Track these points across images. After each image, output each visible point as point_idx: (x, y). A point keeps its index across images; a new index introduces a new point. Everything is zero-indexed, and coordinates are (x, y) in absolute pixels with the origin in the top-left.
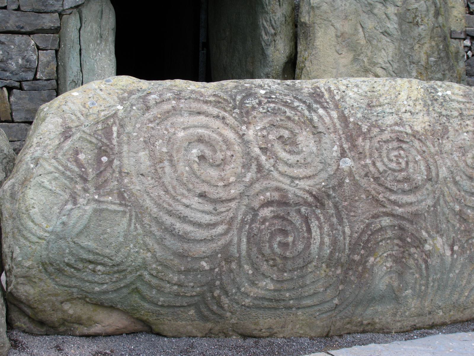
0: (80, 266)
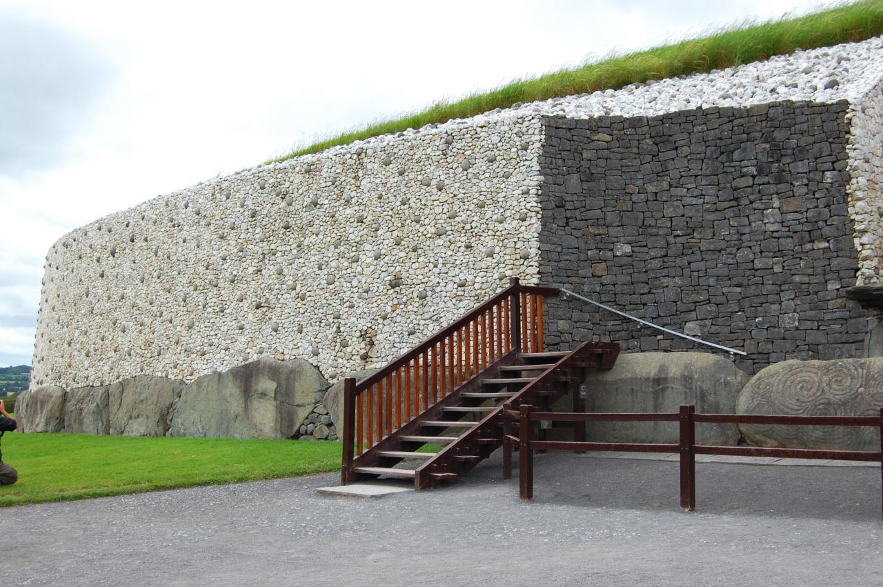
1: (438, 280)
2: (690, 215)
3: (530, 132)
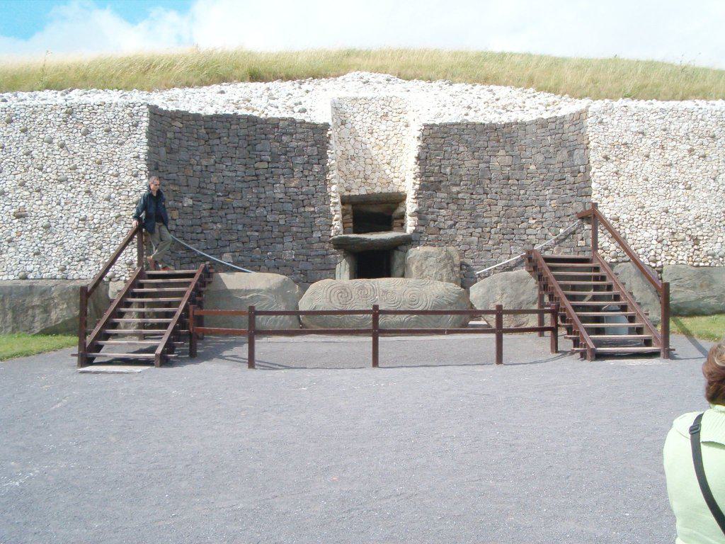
1: (60, 215)
2: (227, 182)
3: (139, 114)
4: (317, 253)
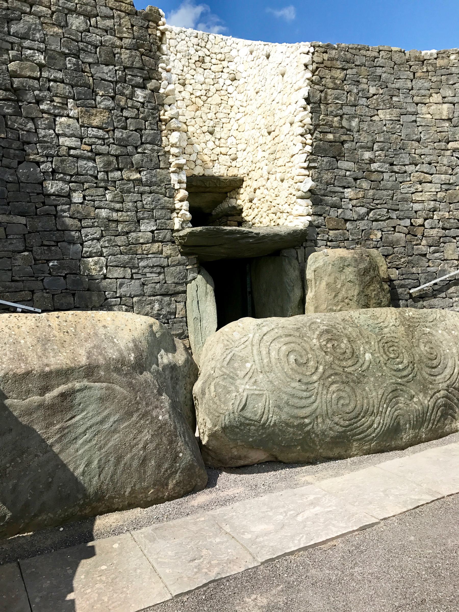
0: (243, 427)
4: (150, 262)
